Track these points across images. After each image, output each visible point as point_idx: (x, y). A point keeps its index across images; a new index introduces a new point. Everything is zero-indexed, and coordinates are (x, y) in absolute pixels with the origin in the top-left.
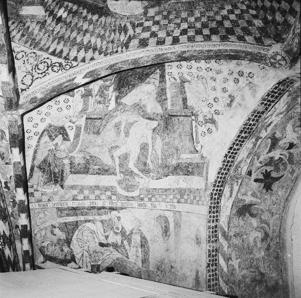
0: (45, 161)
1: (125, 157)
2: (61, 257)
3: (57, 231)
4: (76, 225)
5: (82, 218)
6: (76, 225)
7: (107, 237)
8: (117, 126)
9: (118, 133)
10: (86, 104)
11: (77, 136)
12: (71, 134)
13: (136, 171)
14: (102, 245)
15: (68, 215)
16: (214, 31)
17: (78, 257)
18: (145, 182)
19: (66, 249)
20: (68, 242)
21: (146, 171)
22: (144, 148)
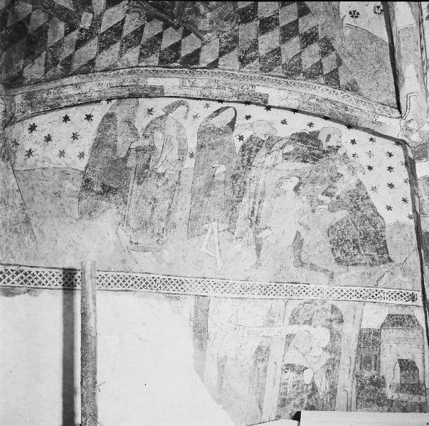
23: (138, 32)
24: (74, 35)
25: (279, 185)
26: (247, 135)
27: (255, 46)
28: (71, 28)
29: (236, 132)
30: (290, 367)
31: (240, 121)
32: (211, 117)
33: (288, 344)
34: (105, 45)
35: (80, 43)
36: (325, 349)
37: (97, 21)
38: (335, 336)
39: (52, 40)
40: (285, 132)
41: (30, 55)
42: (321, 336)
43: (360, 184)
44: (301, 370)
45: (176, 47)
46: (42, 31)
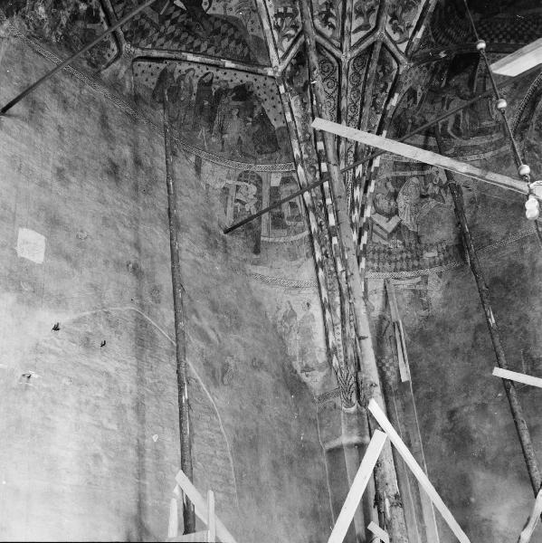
0: (399, 116)
1: (445, 125)
2: (387, 211)
3: (390, 185)
4: (404, 179)
5: (409, 174)
6: (404, 179)
7: (427, 189)
8: (444, 99)
9: (443, 106)
10: (432, 80)
11: (421, 102)
12: (419, 98)
13: (452, 134)
14: (422, 196)
15: (400, 170)
16: (512, 37)
17: (401, 210)
18: (458, 141)
19: (392, 203)
20: (395, 196)
21: (459, 134)
22: (457, 118)
23: (179, 36)
24: (157, 34)
25: (230, 112)
26: (218, 87)
27: (220, 45)
28: (158, 31)
29: (213, 85)
30: (238, 200)
31: (215, 80)
32: (203, 77)
33: (237, 190)
34: (167, 40)
35: (159, 37)
36: (255, 196)
37: (166, 29)
38: (260, 190)
39: (150, 34)
40: (232, 86)
41: (142, 38)
42: (254, 189)
43: (263, 109)
44: (244, 204)
45: (192, 43)
46: (148, 31)
